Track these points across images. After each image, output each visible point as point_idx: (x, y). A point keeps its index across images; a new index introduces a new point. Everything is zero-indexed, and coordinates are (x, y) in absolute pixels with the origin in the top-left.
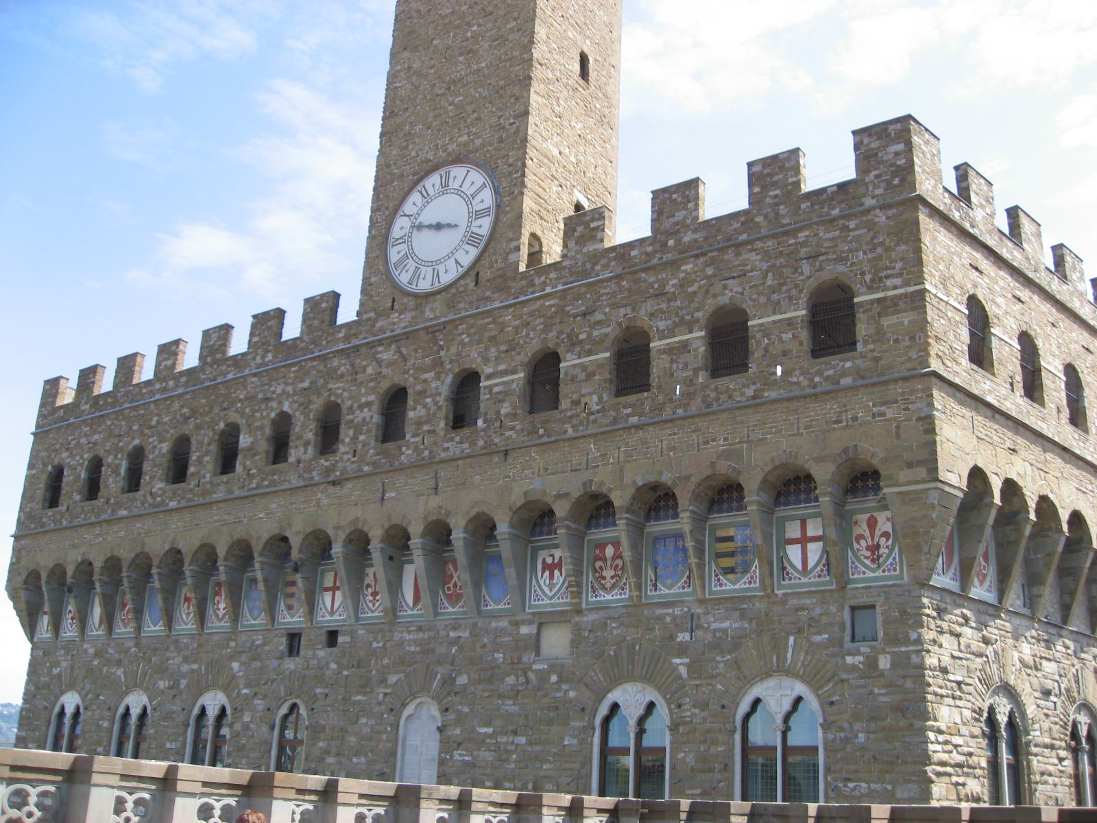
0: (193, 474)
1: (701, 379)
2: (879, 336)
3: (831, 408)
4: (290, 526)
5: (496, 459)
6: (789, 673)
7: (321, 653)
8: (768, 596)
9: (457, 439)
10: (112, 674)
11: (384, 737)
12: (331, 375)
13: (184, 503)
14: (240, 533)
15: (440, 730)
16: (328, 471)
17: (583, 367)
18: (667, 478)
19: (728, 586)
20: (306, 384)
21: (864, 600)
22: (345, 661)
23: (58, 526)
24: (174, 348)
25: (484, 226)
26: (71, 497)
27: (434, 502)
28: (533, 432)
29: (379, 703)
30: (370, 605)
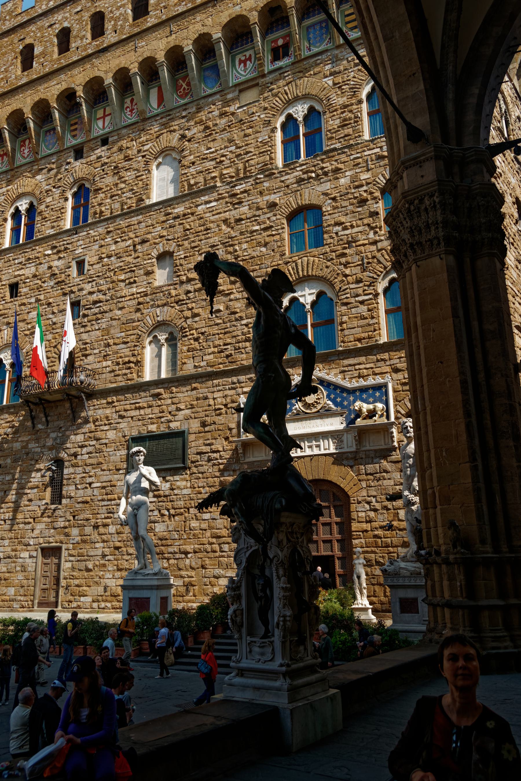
4: (74, 82)
9: (184, 3)
11: (144, 177)
20: (79, 9)
30: (129, 117)
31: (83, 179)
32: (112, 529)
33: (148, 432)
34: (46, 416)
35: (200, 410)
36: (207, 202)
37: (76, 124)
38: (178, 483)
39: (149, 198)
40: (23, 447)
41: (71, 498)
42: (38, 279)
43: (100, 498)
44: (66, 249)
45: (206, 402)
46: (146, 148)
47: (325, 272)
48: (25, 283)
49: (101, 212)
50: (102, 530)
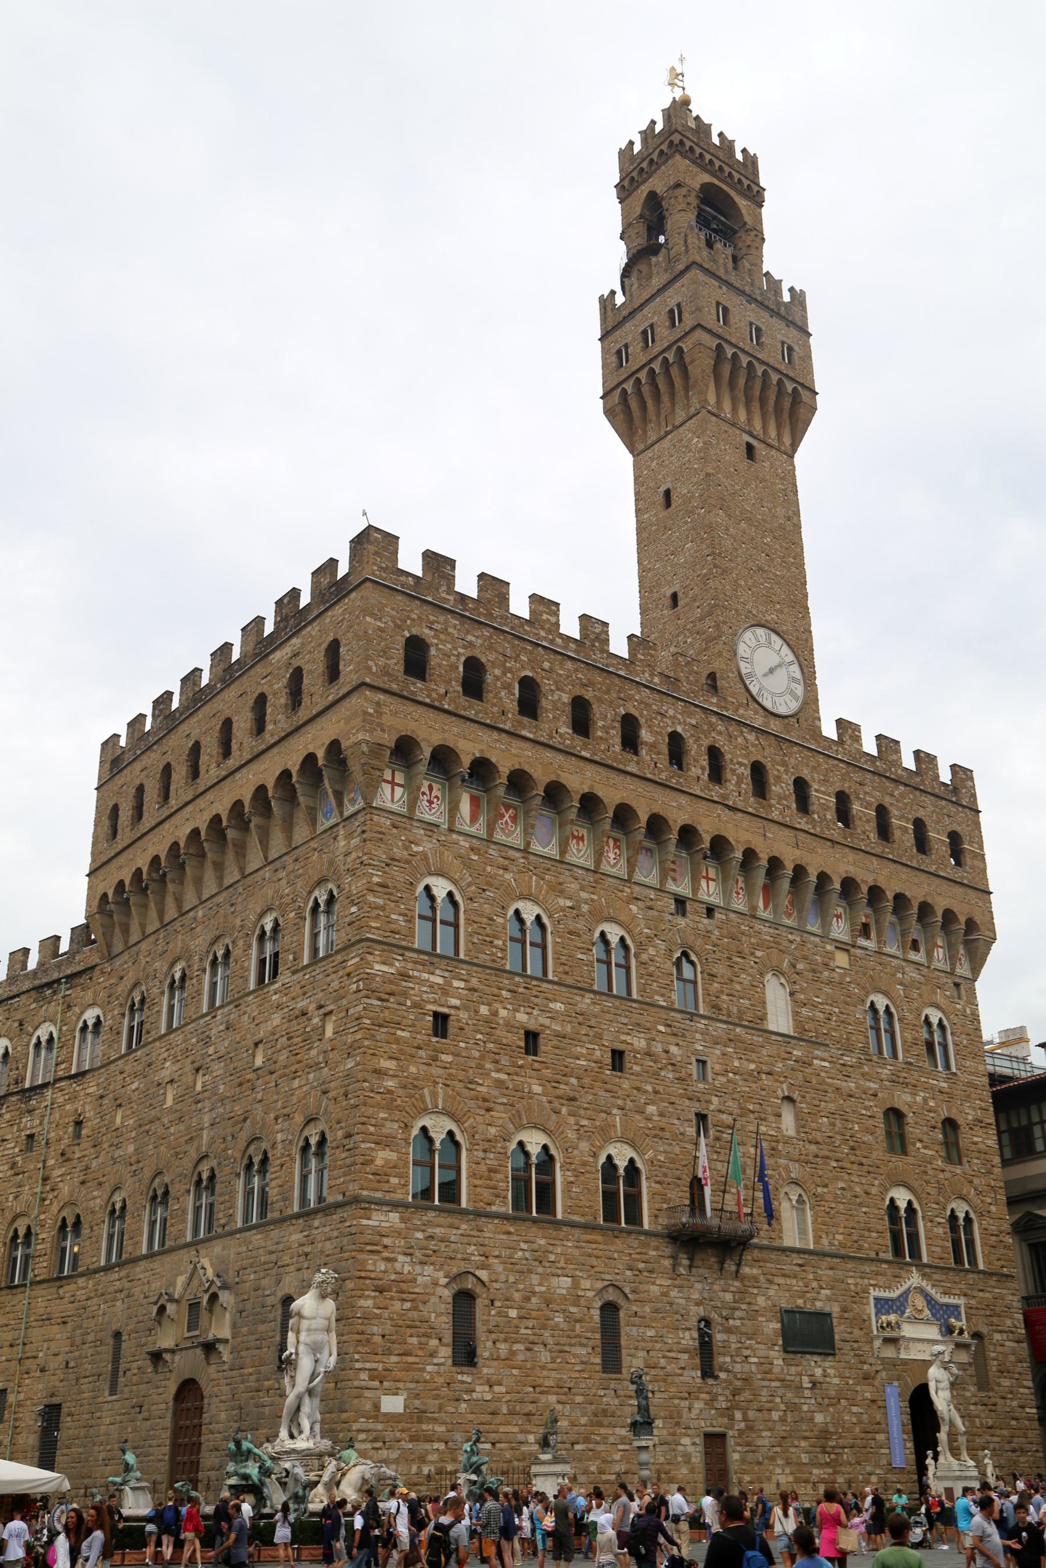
0: (601, 738)
1: (915, 850)
2: (972, 867)
3: (961, 890)
5: (828, 843)
6: (938, 1007)
7: (706, 921)
8: (928, 967)
10: (497, 875)
12: (712, 727)
13: (596, 758)
14: (656, 809)
15: (792, 994)
16: (722, 796)
17: (865, 814)
18: (907, 893)
19: (913, 956)
20: (694, 722)
21: (958, 980)
23: (436, 704)
24: (553, 608)
25: (799, 690)
26: (449, 682)
27: (798, 852)
28: (846, 838)
29: (752, 967)
31: (691, 948)
32: (775, 1415)
33: (797, 1307)
34: (691, 1259)
35: (838, 1292)
37: (673, 862)
38: (829, 1371)
39: (766, 1020)
41: (728, 1371)
42: (652, 1060)
43: (759, 1376)
44: (683, 1036)
45: (843, 1286)
46: (759, 954)
47: (916, 1184)
48: (635, 1057)
49: (717, 1007)
50: (765, 1415)
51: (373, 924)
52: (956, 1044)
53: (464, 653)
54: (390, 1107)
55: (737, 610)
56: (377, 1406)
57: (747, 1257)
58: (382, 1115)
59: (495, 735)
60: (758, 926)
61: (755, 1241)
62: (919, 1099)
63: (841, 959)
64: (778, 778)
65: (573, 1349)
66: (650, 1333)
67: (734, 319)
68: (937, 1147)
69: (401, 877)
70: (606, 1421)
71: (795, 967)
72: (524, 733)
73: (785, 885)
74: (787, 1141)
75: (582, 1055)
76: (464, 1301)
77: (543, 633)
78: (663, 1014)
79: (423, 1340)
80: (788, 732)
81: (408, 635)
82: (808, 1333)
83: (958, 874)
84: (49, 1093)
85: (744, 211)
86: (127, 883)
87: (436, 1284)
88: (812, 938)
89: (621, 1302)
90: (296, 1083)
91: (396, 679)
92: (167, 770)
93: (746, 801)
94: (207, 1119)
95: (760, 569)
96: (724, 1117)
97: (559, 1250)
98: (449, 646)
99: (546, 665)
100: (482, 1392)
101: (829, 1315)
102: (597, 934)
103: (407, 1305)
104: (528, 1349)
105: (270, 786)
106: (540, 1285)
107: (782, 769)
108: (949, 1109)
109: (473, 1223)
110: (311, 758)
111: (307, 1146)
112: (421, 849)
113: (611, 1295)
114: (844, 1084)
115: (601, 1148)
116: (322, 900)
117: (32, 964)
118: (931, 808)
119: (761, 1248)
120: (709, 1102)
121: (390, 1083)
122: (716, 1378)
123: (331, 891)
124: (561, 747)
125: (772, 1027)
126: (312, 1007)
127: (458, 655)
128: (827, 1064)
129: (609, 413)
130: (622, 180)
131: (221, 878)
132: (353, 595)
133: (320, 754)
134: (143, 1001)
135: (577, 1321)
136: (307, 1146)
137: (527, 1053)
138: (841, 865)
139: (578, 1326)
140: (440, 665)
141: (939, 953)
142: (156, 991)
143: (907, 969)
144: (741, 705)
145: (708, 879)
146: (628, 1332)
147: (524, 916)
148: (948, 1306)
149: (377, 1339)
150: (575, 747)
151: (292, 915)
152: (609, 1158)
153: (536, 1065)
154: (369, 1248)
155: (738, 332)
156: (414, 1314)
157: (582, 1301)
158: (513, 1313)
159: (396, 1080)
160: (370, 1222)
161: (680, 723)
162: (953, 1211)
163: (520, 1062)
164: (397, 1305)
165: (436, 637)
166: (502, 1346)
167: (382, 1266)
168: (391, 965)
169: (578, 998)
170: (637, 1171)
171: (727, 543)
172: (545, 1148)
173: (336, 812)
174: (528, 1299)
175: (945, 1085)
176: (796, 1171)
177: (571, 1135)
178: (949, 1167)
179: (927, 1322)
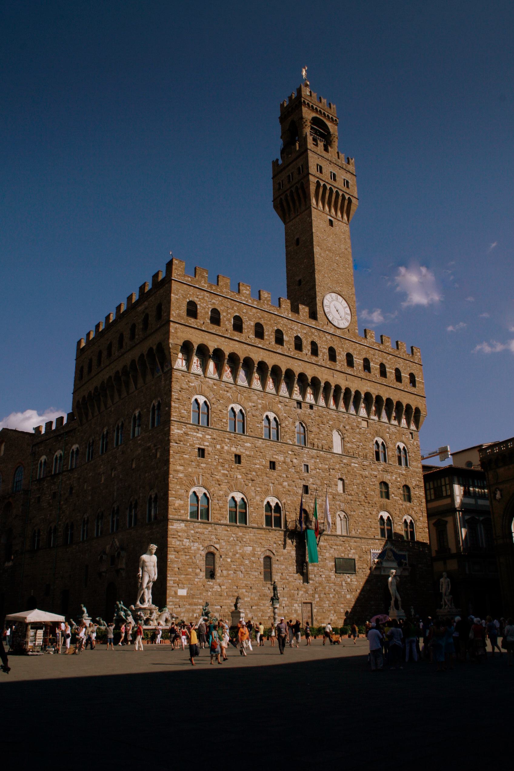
1: (395, 380)
2: (418, 387)
6: (403, 442)
7: (309, 410)
13: (265, 347)
14: (289, 366)
15: (343, 438)
16: (317, 361)
18: (391, 398)
20: (305, 332)
22: (317, 414)
23: (199, 328)
24: (248, 288)
25: (349, 318)
26: (204, 319)
27: (347, 383)
32: (331, 596)
36: (355, 463)
40: (288, 553)
46: (331, 423)
47: (391, 510)
49: (314, 445)
51: (174, 414)
52: (409, 456)
53: (211, 307)
54: (181, 484)
55: (324, 286)
56: (176, 593)
57: (322, 538)
58: (178, 487)
59: (223, 339)
60: (331, 412)
61: (325, 533)
62: (394, 478)
63: (364, 424)
64: (340, 353)
65: (252, 573)
66: (283, 567)
67: (324, 171)
68: (400, 496)
69: (185, 396)
70: (264, 598)
71: (344, 427)
72: (235, 338)
73: (342, 395)
74: (339, 495)
75: (258, 463)
76: (211, 556)
77: (243, 298)
78: (291, 447)
79: (194, 569)
80: (344, 335)
81: (188, 301)
82: (345, 566)
83: (413, 390)
84: (60, 477)
85: (330, 127)
86: (86, 397)
87: (199, 549)
88: (353, 416)
89: (272, 555)
90: (147, 475)
91: (183, 318)
92: (100, 353)
93: (326, 363)
94: (115, 487)
95: (334, 269)
96: (314, 486)
97: (247, 537)
98: (205, 304)
99: (245, 311)
100: (217, 588)
101: (354, 559)
102: (264, 416)
103: (188, 557)
104: (234, 573)
105: (137, 360)
106: (240, 549)
107: (341, 350)
108: (406, 481)
109: (214, 527)
110: (151, 349)
111: (151, 498)
112: (193, 384)
113: (268, 553)
114: (364, 473)
115: (265, 499)
116: (157, 404)
117: (54, 427)
118: (402, 364)
119: (328, 535)
120: (308, 480)
121: (181, 475)
122: (308, 582)
123: (159, 402)
124: (250, 343)
125: (335, 452)
126: (152, 446)
127: (208, 308)
128: (357, 465)
129: (275, 207)
130: (281, 115)
131: (120, 395)
132: (167, 285)
133: (154, 348)
134: (93, 442)
135: (253, 563)
136: (151, 498)
137: (236, 463)
138: (364, 388)
139: (254, 564)
140: (201, 312)
141: (404, 421)
142: (98, 438)
143: (391, 428)
144: (325, 324)
145: (310, 394)
146: (275, 566)
147: (235, 410)
148: (401, 555)
149: (177, 569)
150: (256, 343)
151: (145, 410)
152: (268, 503)
153: (239, 468)
154: (173, 536)
155: (326, 176)
156: (191, 560)
157: (256, 556)
158: (229, 560)
159: (183, 474)
160: (173, 527)
161: (299, 332)
162: (405, 520)
163: (233, 467)
164: (184, 557)
165: (200, 301)
166: (224, 572)
167: (178, 543)
168: (181, 430)
169: (256, 441)
170: (280, 507)
171: (321, 260)
172: (243, 499)
173: (161, 371)
174: (235, 555)
175: (404, 472)
176: (343, 506)
177: (253, 494)
178: (405, 503)
179: (392, 561)
